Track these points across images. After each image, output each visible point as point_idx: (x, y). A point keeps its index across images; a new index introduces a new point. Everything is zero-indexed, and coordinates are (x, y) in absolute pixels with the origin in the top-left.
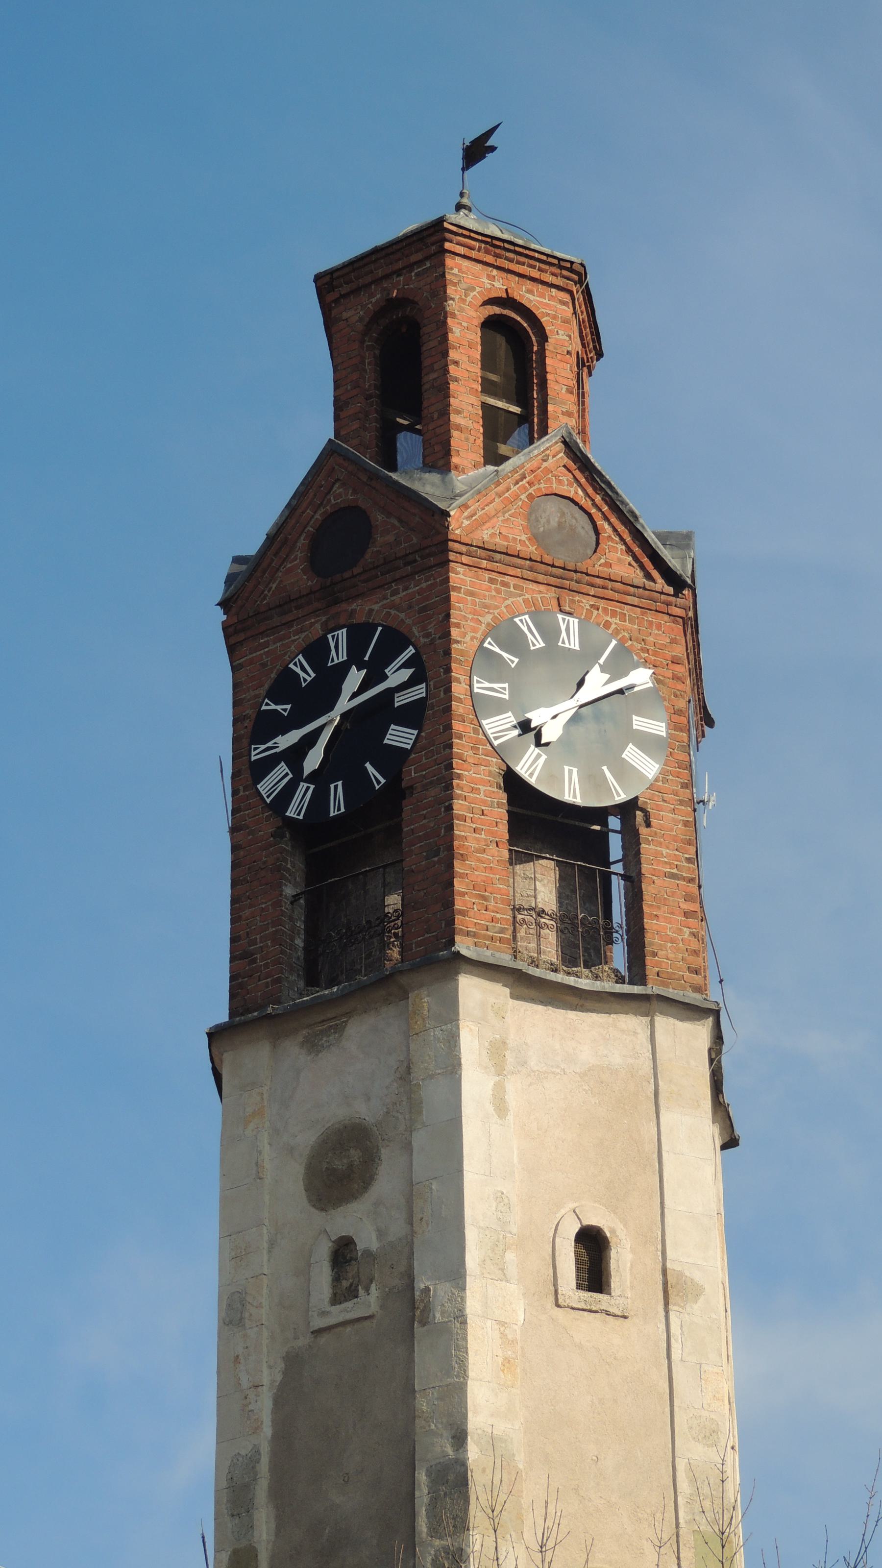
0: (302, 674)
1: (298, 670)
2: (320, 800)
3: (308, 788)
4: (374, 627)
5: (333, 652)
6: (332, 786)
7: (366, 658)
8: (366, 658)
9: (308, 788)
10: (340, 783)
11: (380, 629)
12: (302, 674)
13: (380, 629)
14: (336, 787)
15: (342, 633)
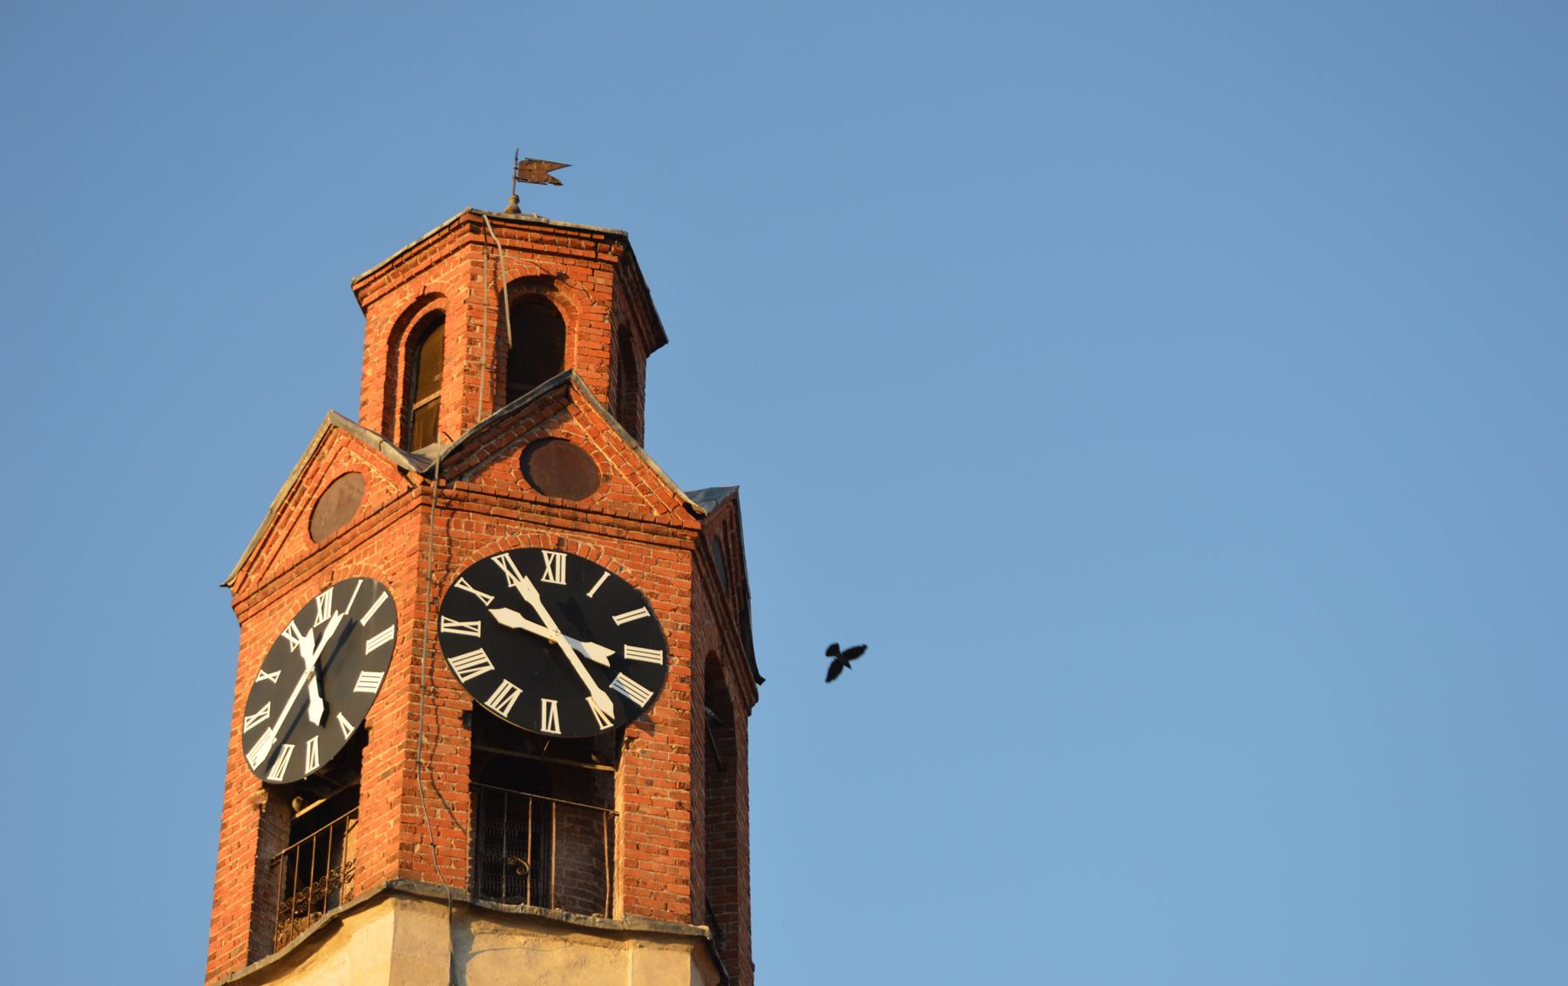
0: (508, 574)
1: (504, 567)
2: (527, 708)
3: (512, 690)
4: (601, 570)
5: (548, 570)
6: (544, 701)
7: (590, 594)
8: (590, 594)
9: (512, 690)
10: (554, 703)
11: (606, 575)
12: (508, 574)
13: (606, 575)
14: (549, 705)
15: (561, 559)
